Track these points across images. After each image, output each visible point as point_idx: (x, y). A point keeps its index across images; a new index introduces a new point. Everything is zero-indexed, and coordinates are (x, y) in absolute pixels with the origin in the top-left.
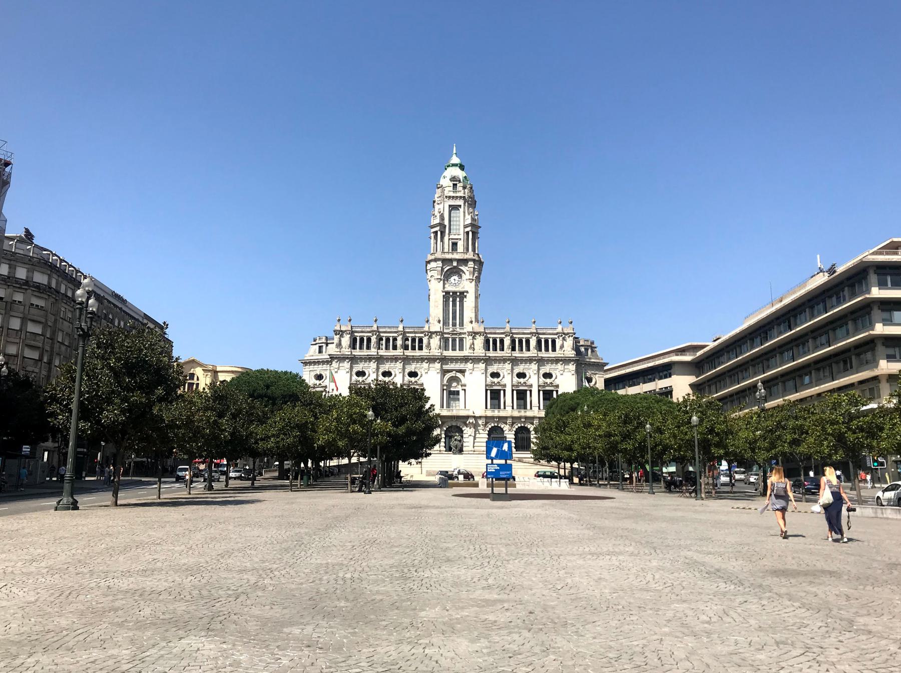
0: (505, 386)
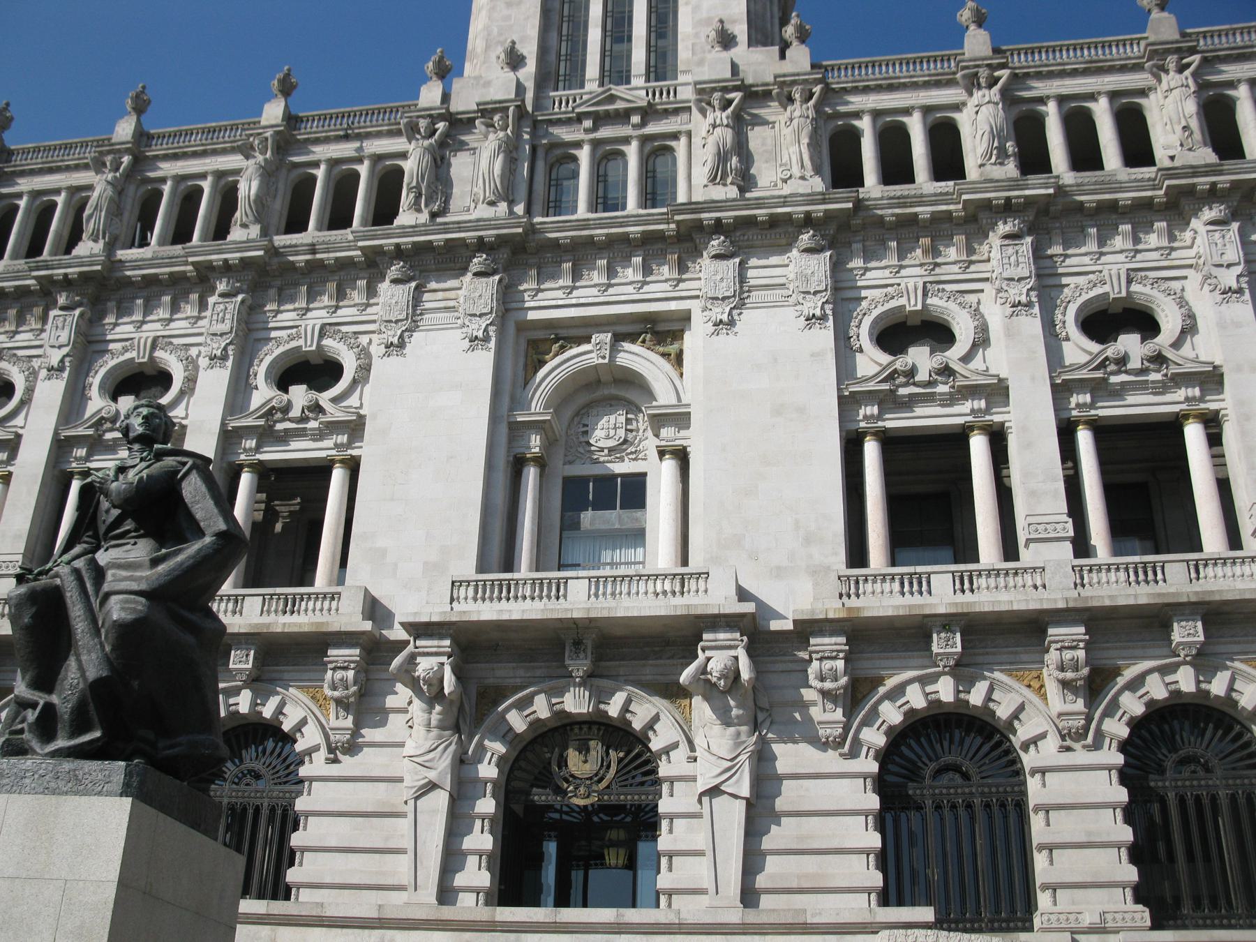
0: (998, 392)
